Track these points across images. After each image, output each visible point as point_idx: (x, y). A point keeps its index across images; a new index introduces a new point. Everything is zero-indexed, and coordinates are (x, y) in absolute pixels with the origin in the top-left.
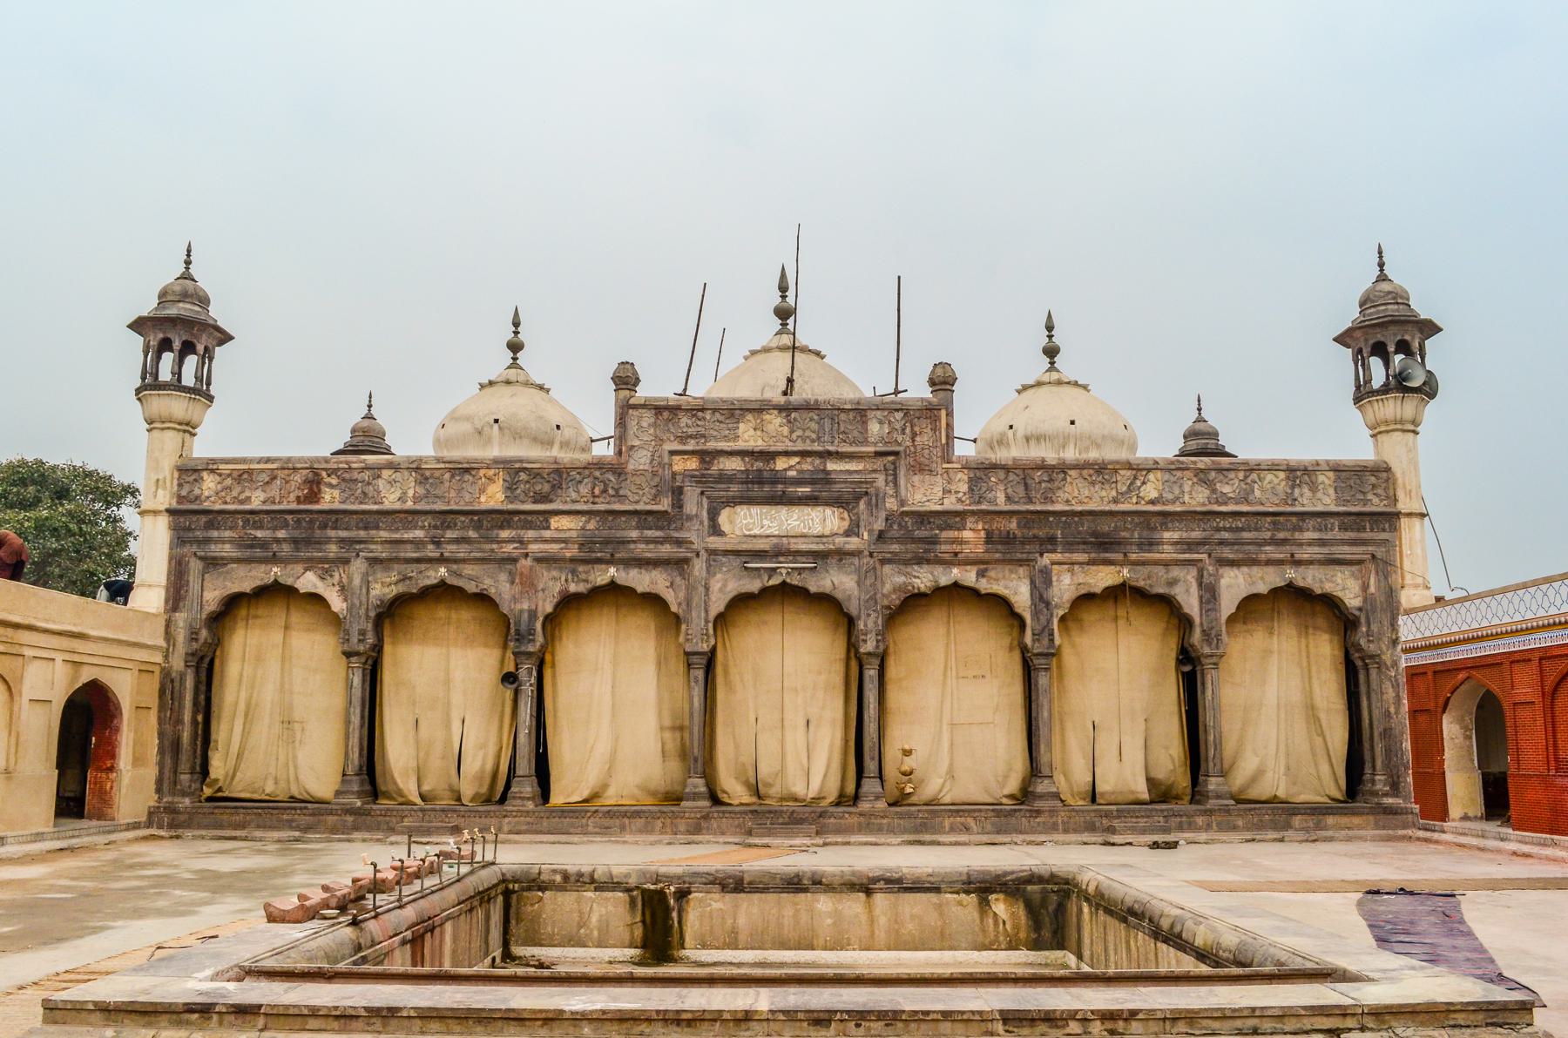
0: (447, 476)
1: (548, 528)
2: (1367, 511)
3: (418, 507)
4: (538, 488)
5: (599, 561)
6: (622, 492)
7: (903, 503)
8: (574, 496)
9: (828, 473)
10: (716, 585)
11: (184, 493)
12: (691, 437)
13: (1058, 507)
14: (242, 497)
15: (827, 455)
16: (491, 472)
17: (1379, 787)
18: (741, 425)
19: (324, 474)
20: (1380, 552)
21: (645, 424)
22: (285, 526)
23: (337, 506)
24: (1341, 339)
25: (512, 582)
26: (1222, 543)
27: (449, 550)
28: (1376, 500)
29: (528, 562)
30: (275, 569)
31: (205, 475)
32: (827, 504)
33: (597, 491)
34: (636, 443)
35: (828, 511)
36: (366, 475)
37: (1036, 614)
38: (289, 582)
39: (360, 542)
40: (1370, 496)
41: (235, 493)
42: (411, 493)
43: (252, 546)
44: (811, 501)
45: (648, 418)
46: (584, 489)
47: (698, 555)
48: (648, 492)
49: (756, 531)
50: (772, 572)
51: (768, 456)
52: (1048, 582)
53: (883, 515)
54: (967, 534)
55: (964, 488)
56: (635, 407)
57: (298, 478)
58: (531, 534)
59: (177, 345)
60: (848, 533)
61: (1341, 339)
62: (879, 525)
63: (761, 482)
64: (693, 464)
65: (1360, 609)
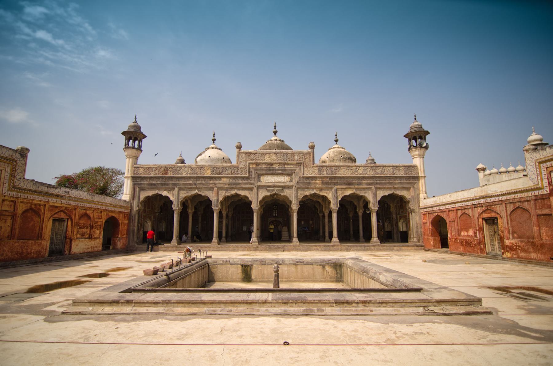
3: (192, 176)
5: (233, 188)
10: (260, 194)
13: (339, 175)
15: (285, 164)
23: (172, 176)
24: (405, 136)
26: (377, 183)
32: (285, 175)
45: (244, 155)
46: (229, 172)
48: (244, 173)
51: (272, 164)
54: (318, 182)
55: (317, 171)
56: (241, 153)
57: (162, 169)
58: (217, 182)
59: (133, 138)
60: (290, 182)
61: (405, 136)
63: (270, 170)
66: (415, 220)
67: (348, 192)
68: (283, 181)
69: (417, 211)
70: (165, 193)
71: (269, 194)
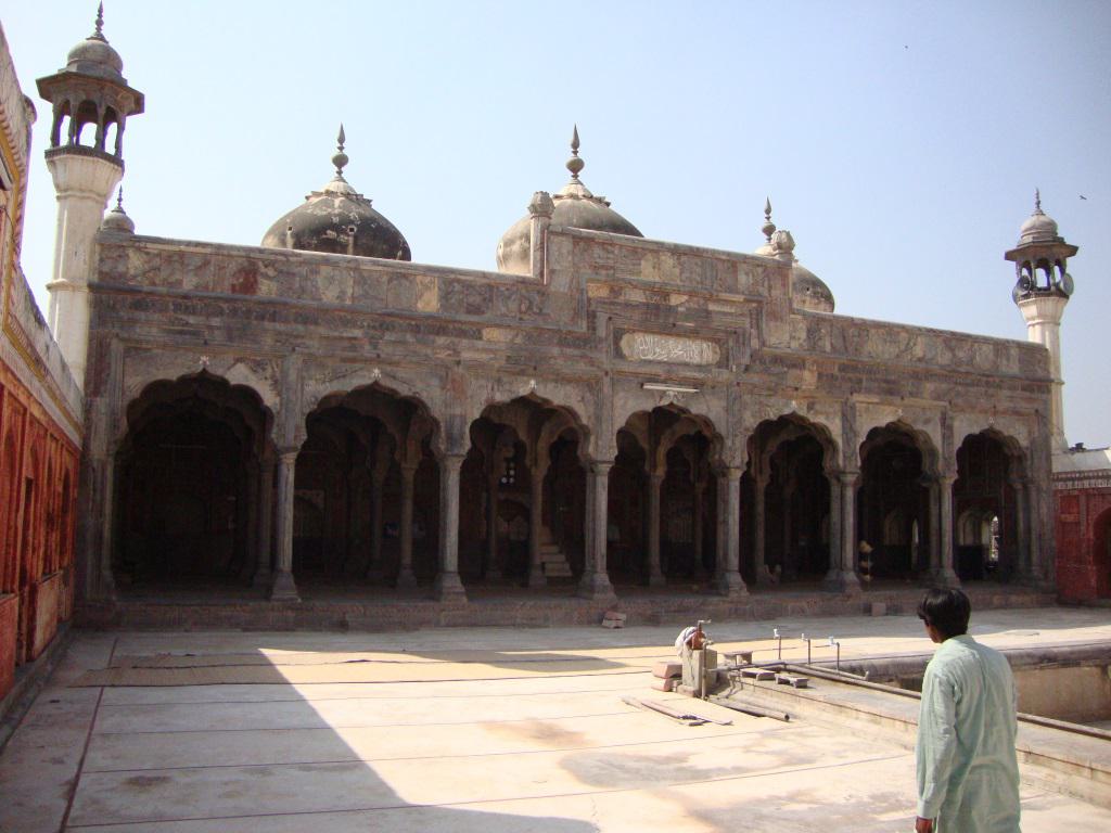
0: (385, 279)
1: (481, 338)
2: (1032, 374)
4: (471, 300)
5: (522, 373)
6: (545, 311)
7: (763, 344)
8: (504, 310)
9: (708, 313)
10: (619, 402)
11: (106, 269)
12: (603, 267)
14: (173, 279)
16: (428, 279)
17: (1035, 574)
18: (643, 262)
19: (260, 264)
20: (1041, 408)
21: (564, 251)
22: (221, 313)
24: (1009, 256)
25: (443, 388)
27: (386, 350)
28: (1039, 370)
29: (460, 370)
30: (204, 358)
31: (131, 252)
33: (523, 308)
34: (557, 267)
35: (705, 345)
36: (304, 270)
37: (847, 441)
38: (220, 372)
39: (297, 337)
40: (1036, 367)
41: (164, 274)
42: (350, 291)
43: (181, 333)
44: (693, 334)
45: (567, 245)
46: (513, 306)
47: (607, 373)
49: (650, 357)
50: (663, 394)
52: (854, 417)
53: (748, 352)
54: (807, 374)
57: (233, 267)
59: (102, 111)
61: (1009, 256)
62: (746, 360)
64: (604, 293)
65: (1027, 448)
66: (1042, 511)
67: (885, 417)
68: (697, 360)
69: (1044, 485)
70: (238, 375)
71: (649, 406)
